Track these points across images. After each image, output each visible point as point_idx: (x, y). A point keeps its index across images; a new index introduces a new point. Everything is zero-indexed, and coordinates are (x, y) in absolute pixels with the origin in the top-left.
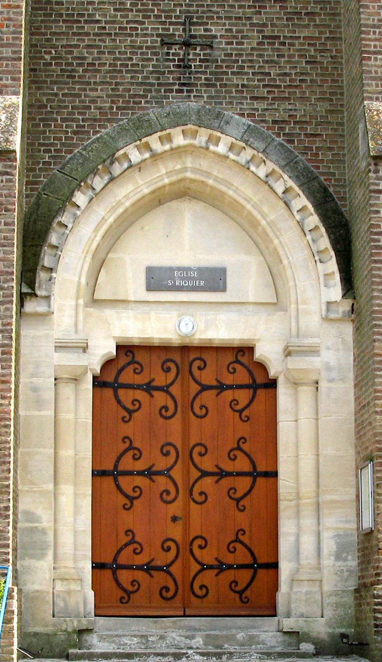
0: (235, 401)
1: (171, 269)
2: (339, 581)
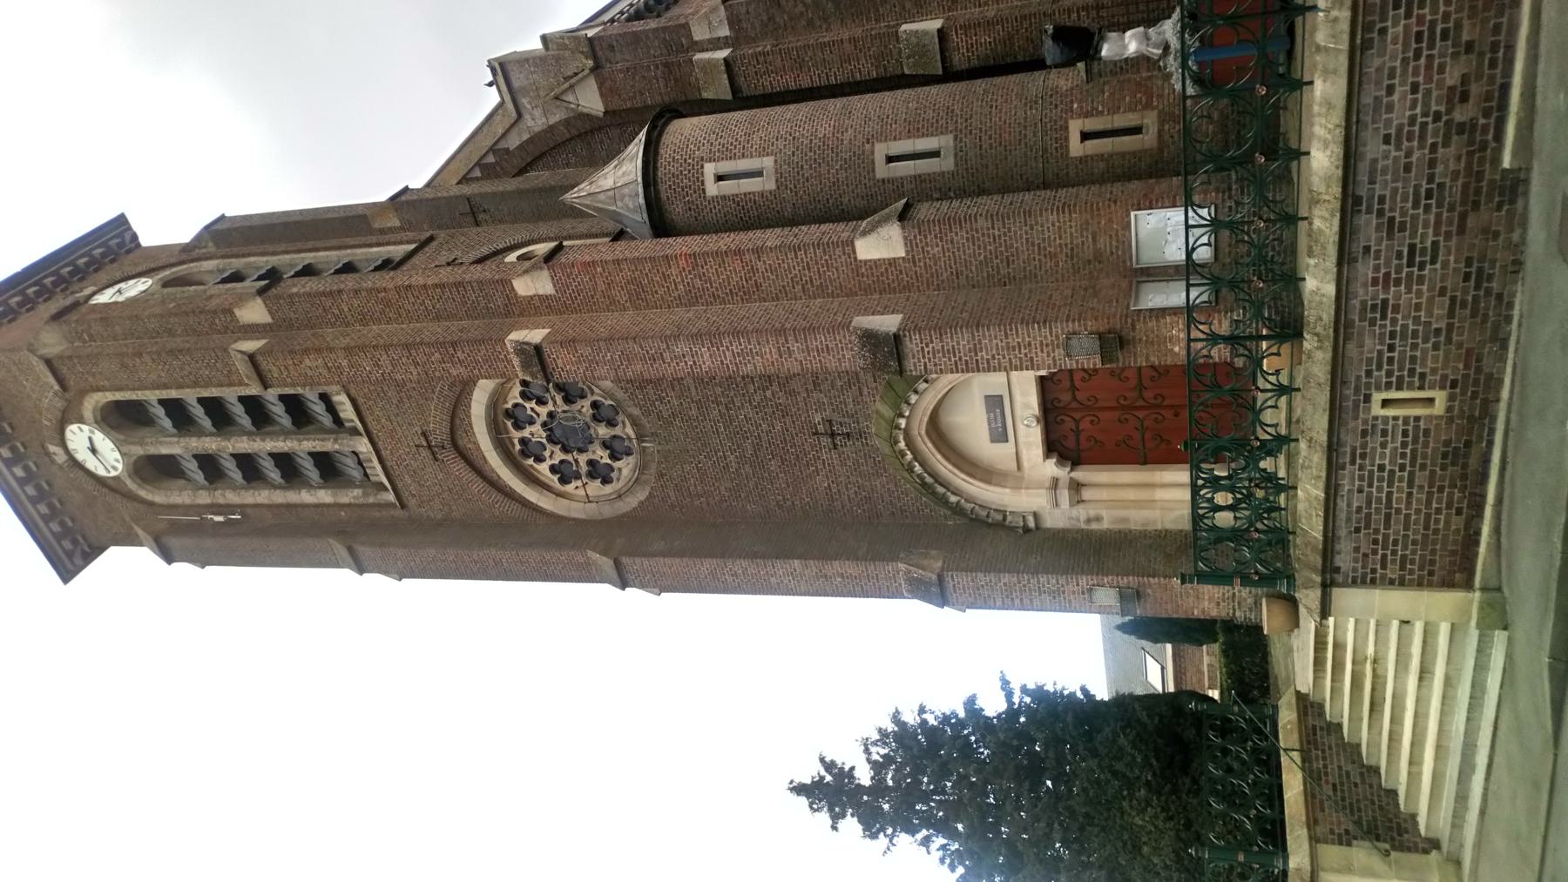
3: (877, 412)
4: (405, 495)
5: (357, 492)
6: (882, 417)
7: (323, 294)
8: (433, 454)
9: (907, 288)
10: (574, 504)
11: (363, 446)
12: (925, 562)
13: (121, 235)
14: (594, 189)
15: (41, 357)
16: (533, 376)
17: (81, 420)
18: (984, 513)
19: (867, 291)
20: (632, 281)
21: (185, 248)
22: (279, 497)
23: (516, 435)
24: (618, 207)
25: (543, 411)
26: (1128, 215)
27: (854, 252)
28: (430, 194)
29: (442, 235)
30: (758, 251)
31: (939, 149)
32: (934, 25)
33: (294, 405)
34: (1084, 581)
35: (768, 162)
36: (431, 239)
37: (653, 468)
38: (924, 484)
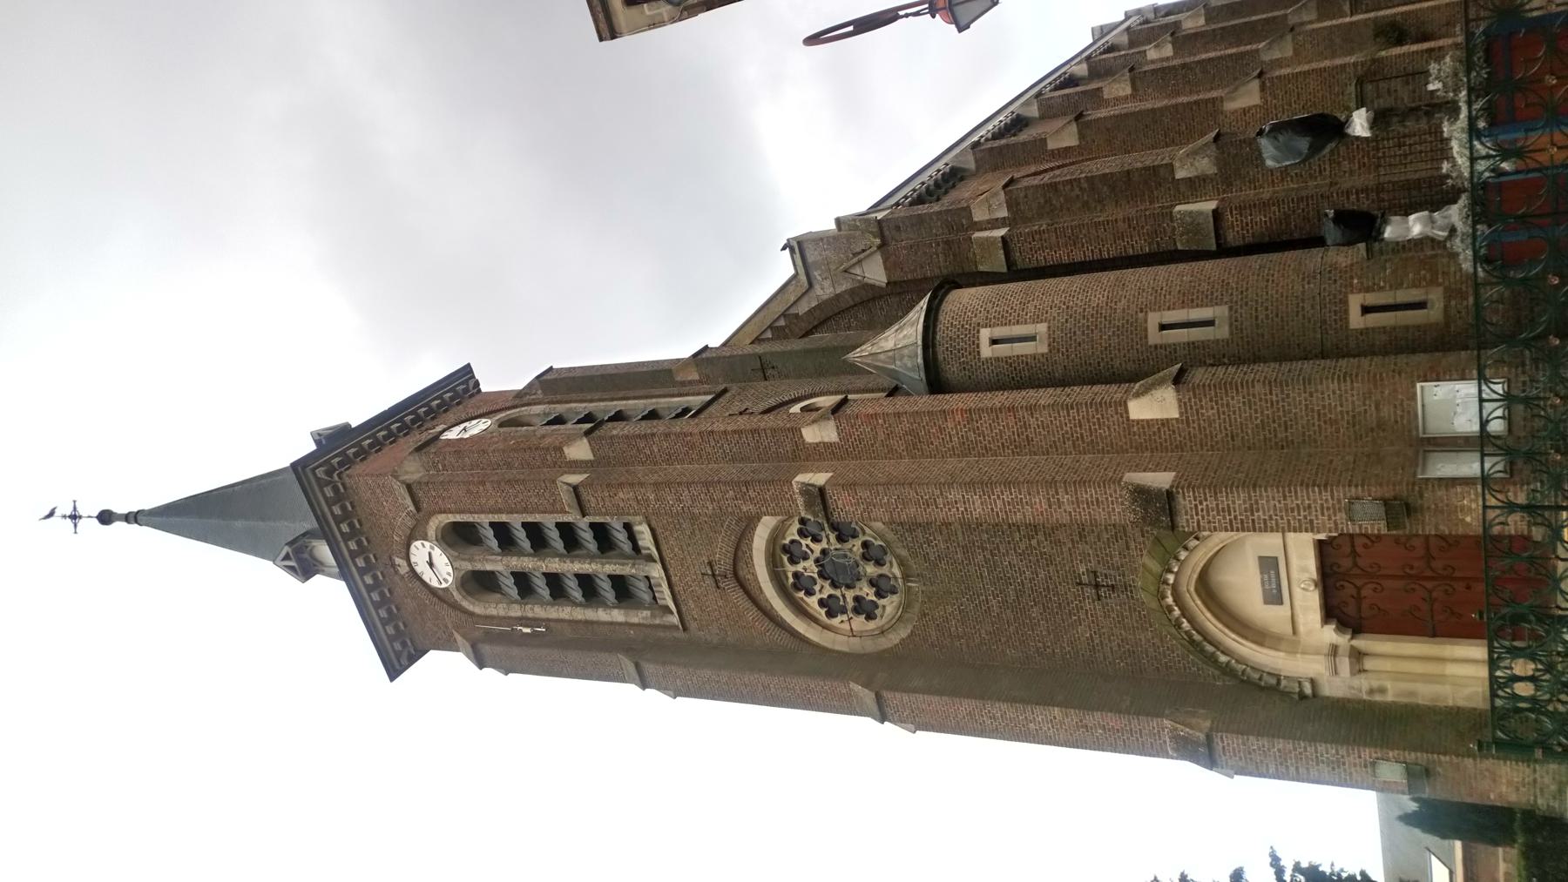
0: (1365, 546)
1: (1264, 591)
2: (1471, 141)
3: (1144, 566)
4: (687, 618)
5: (646, 613)
6: (1150, 572)
7: (639, 436)
8: (716, 582)
9: (1180, 447)
10: (839, 637)
11: (656, 572)
12: (1194, 721)
13: (466, 382)
14: (875, 350)
15: (403, 482)
16: (815, 515)
17: (425, 538)
18: (1256, 676)
19: (1139, 448)
20: (911, 432)
21: (519, 394)
22: (580, 614)
23: (790, 569)
24: (897, 366)
25: (817, 548)
26: (1414, 387)
27: (1127, 412)
28: (727, 352)
29: (734, 388)
30: (1031, 409)
31: (1213, 320)
32: (1211, 205)
33: (601, 531)
34: (1367, 753)
35: (1042, 328)
36: (725, 391)
37: (917, 608)
38: (1192, 641)
